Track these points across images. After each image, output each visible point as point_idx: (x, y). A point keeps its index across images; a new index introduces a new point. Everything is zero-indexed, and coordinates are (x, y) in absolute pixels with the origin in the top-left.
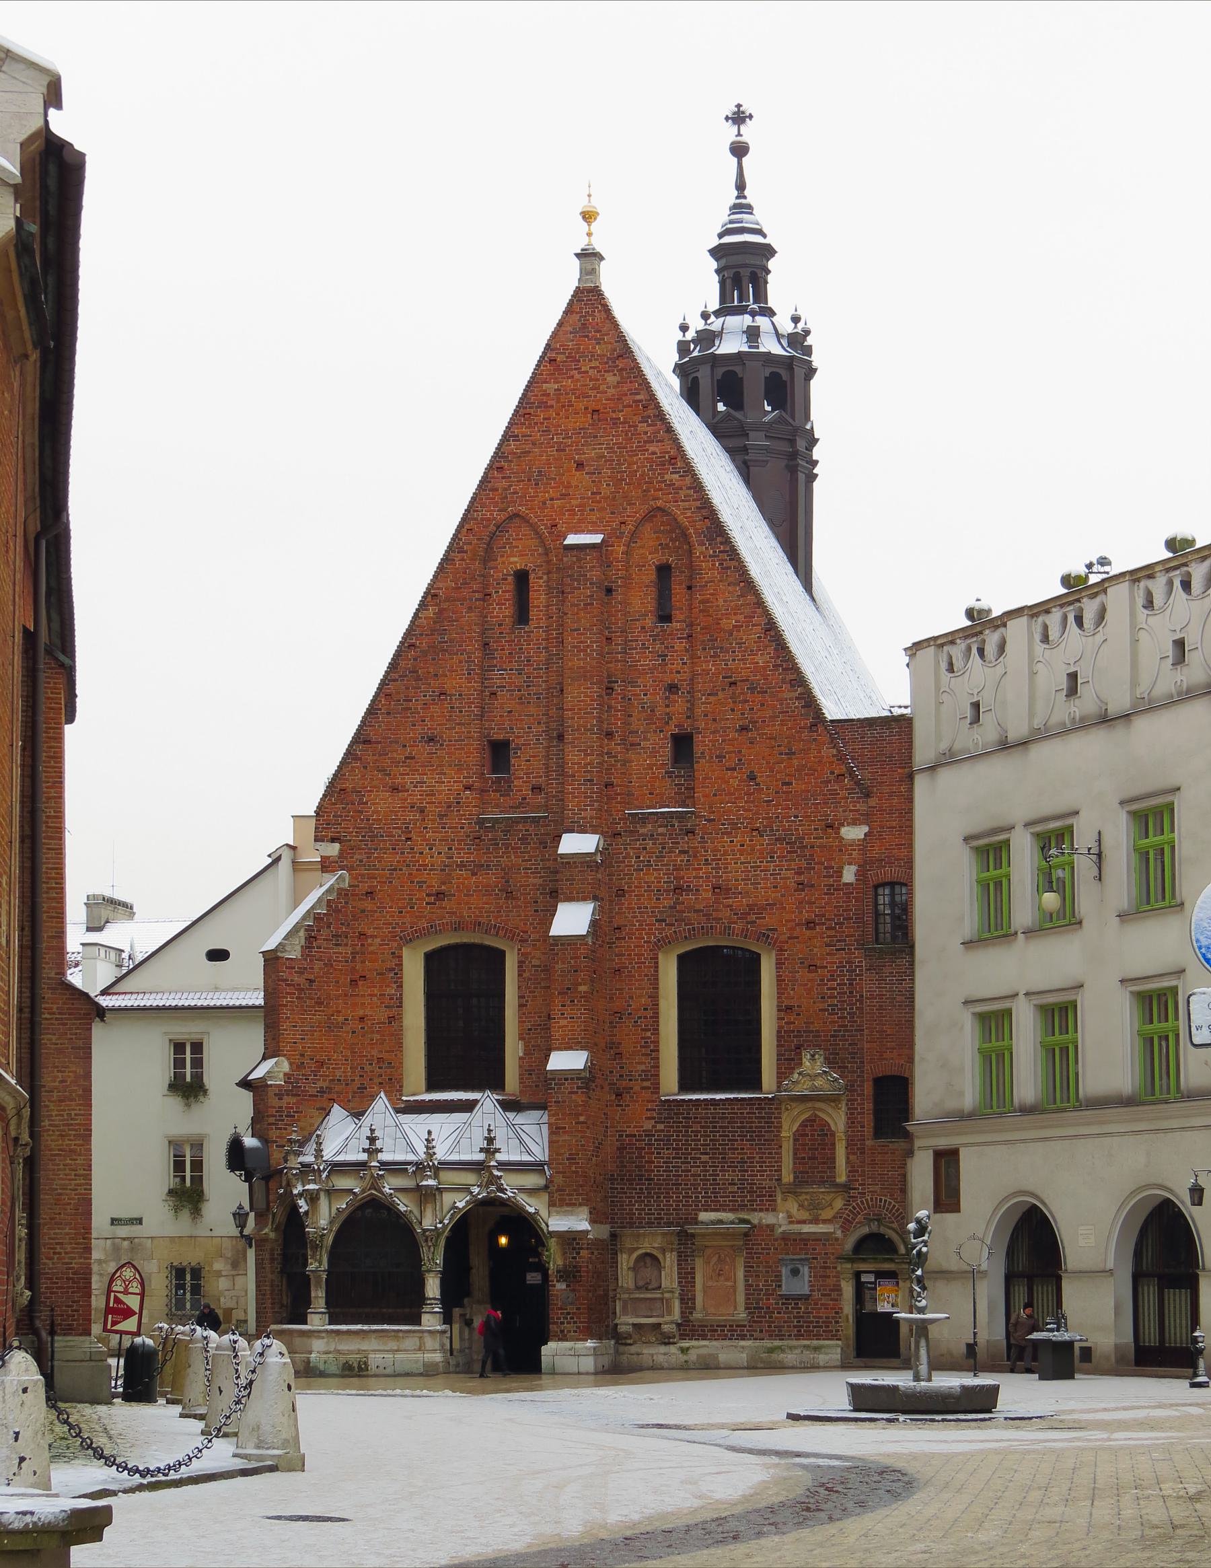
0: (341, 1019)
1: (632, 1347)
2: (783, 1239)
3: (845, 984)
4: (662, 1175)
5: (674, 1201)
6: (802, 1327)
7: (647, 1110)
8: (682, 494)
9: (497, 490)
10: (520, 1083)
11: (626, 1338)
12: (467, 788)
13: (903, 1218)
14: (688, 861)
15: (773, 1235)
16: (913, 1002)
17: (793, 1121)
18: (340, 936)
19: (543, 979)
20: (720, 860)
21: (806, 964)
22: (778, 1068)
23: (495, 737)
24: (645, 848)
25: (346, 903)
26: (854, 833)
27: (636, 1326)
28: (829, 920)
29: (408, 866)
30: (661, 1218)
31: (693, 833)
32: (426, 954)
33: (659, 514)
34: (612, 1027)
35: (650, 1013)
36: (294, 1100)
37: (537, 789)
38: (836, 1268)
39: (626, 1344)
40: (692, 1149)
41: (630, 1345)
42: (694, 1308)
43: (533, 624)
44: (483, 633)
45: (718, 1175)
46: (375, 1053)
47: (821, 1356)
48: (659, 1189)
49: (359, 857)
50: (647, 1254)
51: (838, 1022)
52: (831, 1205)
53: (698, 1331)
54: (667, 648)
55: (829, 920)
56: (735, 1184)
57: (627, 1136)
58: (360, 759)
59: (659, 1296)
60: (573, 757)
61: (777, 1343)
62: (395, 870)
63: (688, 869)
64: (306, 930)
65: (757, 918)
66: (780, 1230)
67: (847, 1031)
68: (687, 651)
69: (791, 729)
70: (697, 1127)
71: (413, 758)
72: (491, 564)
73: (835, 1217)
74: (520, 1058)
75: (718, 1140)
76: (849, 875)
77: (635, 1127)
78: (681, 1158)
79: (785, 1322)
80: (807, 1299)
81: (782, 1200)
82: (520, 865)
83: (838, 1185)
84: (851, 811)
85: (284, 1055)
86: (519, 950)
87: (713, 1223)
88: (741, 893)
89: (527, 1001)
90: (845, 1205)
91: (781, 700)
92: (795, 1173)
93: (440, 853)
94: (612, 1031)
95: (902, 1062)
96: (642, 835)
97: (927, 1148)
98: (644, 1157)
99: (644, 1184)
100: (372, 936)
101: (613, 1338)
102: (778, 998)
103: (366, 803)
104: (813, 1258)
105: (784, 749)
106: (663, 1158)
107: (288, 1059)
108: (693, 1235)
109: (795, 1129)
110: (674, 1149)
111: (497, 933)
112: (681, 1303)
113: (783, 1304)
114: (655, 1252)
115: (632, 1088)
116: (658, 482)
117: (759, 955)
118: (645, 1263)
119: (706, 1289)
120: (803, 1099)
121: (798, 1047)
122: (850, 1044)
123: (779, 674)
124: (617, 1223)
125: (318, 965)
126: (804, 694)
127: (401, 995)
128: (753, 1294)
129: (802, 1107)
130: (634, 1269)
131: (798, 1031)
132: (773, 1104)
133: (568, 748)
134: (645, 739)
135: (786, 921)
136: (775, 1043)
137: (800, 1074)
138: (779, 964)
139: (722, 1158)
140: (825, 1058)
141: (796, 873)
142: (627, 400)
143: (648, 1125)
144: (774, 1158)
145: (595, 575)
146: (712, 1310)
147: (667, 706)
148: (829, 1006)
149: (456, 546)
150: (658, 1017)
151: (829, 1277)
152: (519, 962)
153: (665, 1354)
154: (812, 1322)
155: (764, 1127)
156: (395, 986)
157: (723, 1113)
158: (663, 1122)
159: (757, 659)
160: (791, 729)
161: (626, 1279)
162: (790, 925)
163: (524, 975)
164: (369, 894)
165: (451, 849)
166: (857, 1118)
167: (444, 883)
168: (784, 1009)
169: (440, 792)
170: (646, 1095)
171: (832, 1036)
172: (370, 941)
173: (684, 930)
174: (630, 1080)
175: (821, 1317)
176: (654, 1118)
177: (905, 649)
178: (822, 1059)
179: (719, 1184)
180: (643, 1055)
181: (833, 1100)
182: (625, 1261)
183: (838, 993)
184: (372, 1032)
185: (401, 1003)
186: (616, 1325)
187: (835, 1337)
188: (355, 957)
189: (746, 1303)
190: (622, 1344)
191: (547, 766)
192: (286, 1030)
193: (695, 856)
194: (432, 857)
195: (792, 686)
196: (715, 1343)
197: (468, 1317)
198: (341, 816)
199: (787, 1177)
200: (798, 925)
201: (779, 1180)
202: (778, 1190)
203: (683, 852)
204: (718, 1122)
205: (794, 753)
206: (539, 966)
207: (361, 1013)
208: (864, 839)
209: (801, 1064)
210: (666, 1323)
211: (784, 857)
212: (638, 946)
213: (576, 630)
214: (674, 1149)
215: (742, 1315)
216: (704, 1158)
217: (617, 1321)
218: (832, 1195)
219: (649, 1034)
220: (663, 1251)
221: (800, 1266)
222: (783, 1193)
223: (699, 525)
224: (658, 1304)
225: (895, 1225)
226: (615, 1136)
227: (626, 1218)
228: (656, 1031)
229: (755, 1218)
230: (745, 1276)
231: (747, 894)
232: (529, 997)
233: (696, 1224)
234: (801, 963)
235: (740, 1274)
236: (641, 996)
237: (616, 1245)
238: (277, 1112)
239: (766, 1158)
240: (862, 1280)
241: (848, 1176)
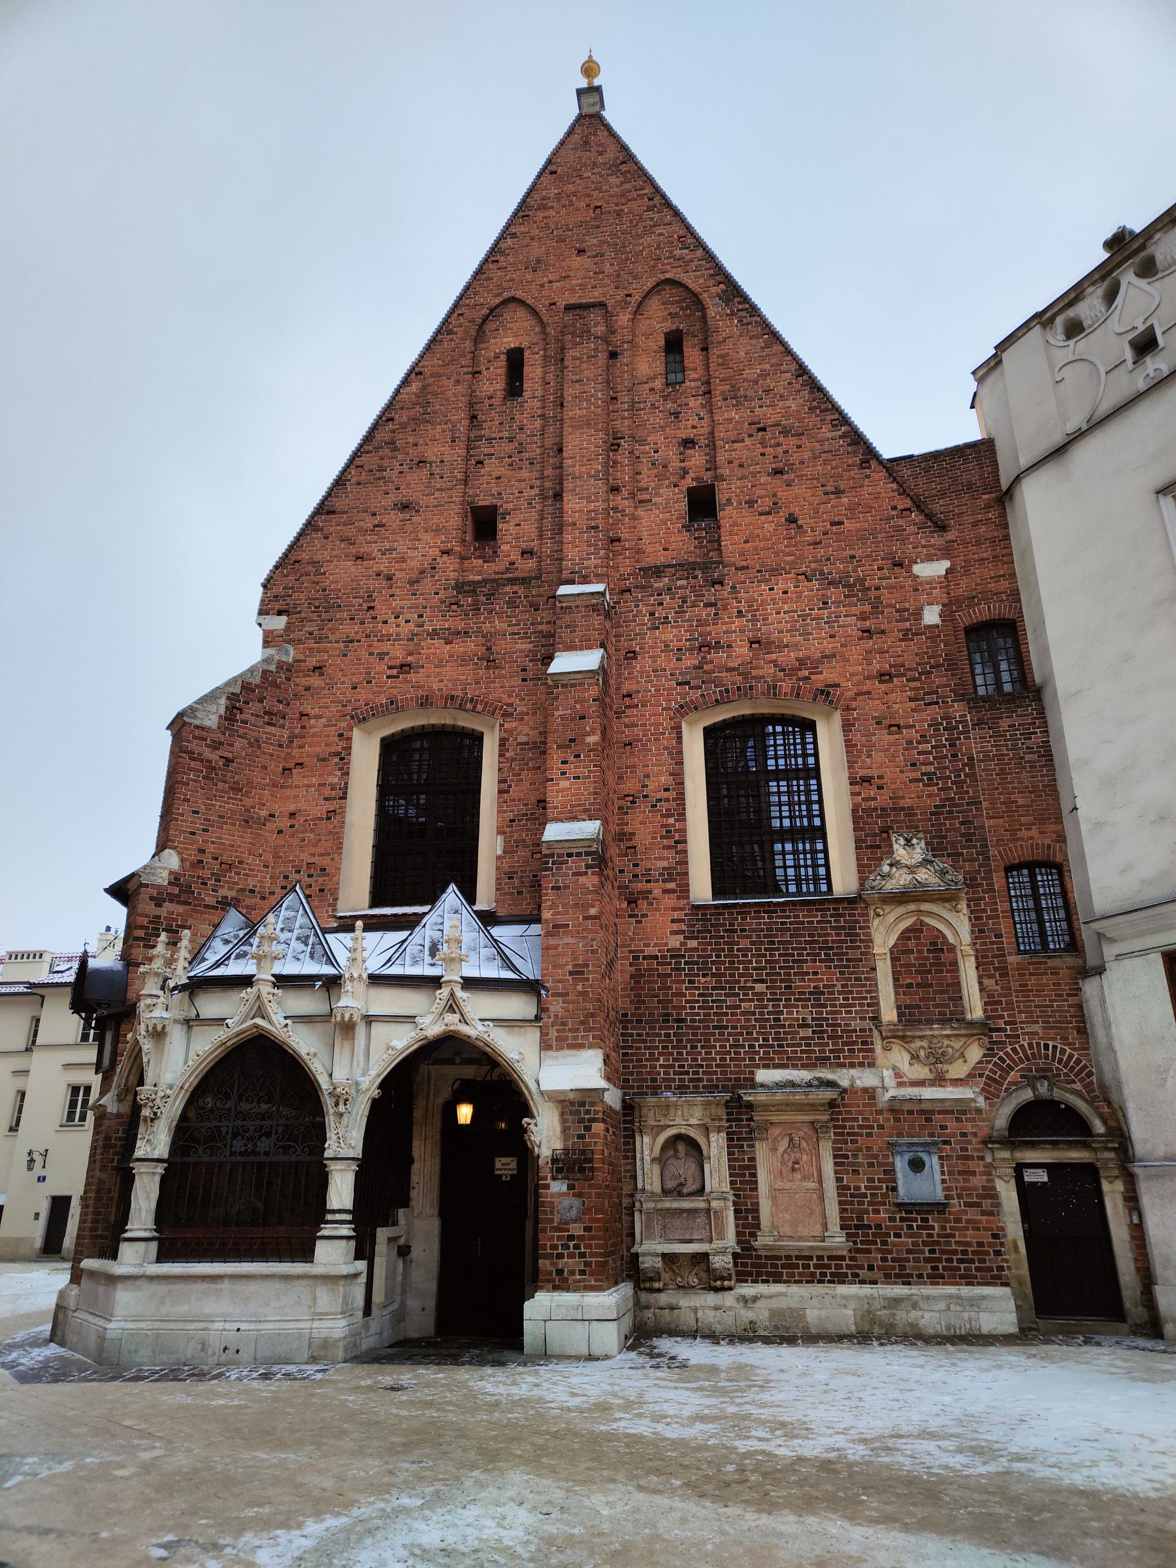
0: (264, 813)
1: (662, 1295)
2: (892, 1111)
3: (945, 746)
4: (698, 1014)
5: (717, 1053)
6: (939, 1260)
7: (673, 921)
8: (693, 265)
9: (491, 279)
10: (497, 889)
11: (651, 1279)
12: (447, 552)
13: (1090, 1074)
14: (715, 614)
15: (874, 1105)
16: (1052, 760)
17: (889, 930)
18: (275, 715)
19: (531, 759)
20: (758, 610)
21: (886, 722)
22: (858, 859)
23: (481, 503)
24: (661, 604)
25: (288, 679)
26: (932, 570)
27: (668, 1258)
28: (910, 670)
29: (368, 636)
30: (700, 1080)
31: (721, 583)
32: (383, 740)
33: (667, 287)
34: (621, 814)
35: (672, 794)
36: (180, 909)
37: (527, 553)
38: (982, 1158)
39: (652, 1290)
40: (741, 975)
41: (659, 1291)
42: (758, 1227)
43: (527, 395)
44: (471, 405)
45: (782, 1013)
46: (305, 857)
47: (983, 1317)
48: (694, 1034)
49: (310, 629)
50: (678, 1137)
51: (937, 795)
52: (962, 1055)
53: (765, 1266)
54: (680, 406)
55: (910, 670)
56: (808, 1026)
57: (645, 958)
58: (322, 530)
59: (702, 1205)
60: (572, 504)
61: (899, 1290)
62: (352, 641)
63: (717, 624)
64: (228, 698)
65: (810, 673)
66: (888, 1096)
67: (956, 805)
68: (703, 406)
69: (836, 468)
70: (744, 943)
71: (383, 526)
72: (482, 346)
73: (971, 1076)
74: (498, 858)
75: (778, 962)
76: (931, 616)
77: (656, 945)
78: (724, 988)
79: (909, 1251)
80: (943, 1212)
81: (886, 1049)
82: (505, 631)
83: (971, 1024)
84: (923, 546)
85: (174, 848)
86: (501, 725)
87: (779, 1085)
88: (787, 646)
89: (510, 786)
90: (985, 1056)
91: (821, 442)
92: (898, 1007)
93: (407, 621)
94: (622, 819)
95: (1047, 841)
96: (658, 589)
97: (1145, 952)
98: (670, 988)
99: (672, 1028)
100: (317, 717)
101: (629, 1277)
102: (849, 768)
103: (324, 573)
104: (945, 1142)
105: (829, 489)
106: (698, 988)
107: (179, 853)
108: (750, 1106)
109: (892, 942)
110: (713, 975)
111: (475, 707)
112: (736, 1218)
113: (902, 1219)
114: (693, 1133)
115: (650, 892)
116: (668, 258)
117: (814, 722)
118: (676, 1151)
119: (774, 1194)
120: (901, 898)
121: (885, 830)
122: (962, 823)
123: (817, 416)
124: (632, 1087)
125: (239, 743)
126: (848, 432)
127: (346, 783)
128: (852, 1203)
129: (901, 910)
130: (661, 1161)
131: (883, 809)
132: (856, 909)
133: (567, 497)
134: (657, 495)
135: (852, 675)
136: (851, 826)
137: (891, 865)
138: (847, 726)
139: (786, 987)
140: (926, 844)
141: (858, 619)
142: (634, 194)
143: (675, 942)
144: (865, 985)
145: (600, 329)
146: (786, 1230)
147: (683, 461)
148: (923, 774)
149: (445, 329)
150: (684, 799)
151: (974, 1173)
152: (500, 740)
153: (716, 1308)
154: (955, 1252)
155: (845, 942)
156: (339, 773)
157: (782, 923)
158: (697, 938)
159: (788, 403)
160: (836, 468)
161: (649, 1178)
162: (855, 679)
163: (507, 755)
164: (318, 669)
165: (420, 616)
166: (986, 924)
167: (411, 654)
168: (858, 781)
169: (413, 558)
170: (669, 901)
171: (932, 814)
172: (313, 721)
173: (715, 692)
174: (648, 881)
175: (969, 1244)
176: (683, 932)
177: (974, 373)
178: (923, 844)
179: (784, 1026)
180: (665, 848)
181: (947, 898)
182: (647, 1147)
183: (934, 758)
184: (305, 831)
185: (345, 793)
186: (637, 1255)
187: (997, 1278)
188: (292, 742)
189: (841, 1218)
190: (645, 1289)
191: (541, 530)
192: (183, 815)
193: (725, 608)
194: (398, 626)
195: (834, 426)
196: (794, 1289)
197: (402, 1241)
198: (292, 588)
199: (889, 1014)
200: (869, 678)
201: (876, 1019)
202: (876, 1033)
203: (707, 605)
204: (776, 936)
205: (843, 492)
206: (526, 743)
207: (292, 808)
208: (946, 577)
209: (891, 852)
210: (718, 1253)
211: (840, 602)
212: (655, 715)
213: (577, 381)
214: (713, 975)
215: (837, 1240)
216: (760, 988)
217: (636, 1249)
218: (963, 1040)
219: (671, 821)
220: (706, 1130)
221: (925, 1156)
222: (883, 1039)
223: (713, 290)
224: (701, 1220)
225: (1078, 1086)
226: (627, 958)
227: (646, 1080)
228: (682, 816)
229: (844, 1077)
230: (836, 1172)
231: (796, 646)
232: (512, 780)
233: (753, 1086)
234: (877, 723)
235: (828, 1167)
236: (659, 774)
237: (632, 1122)
238: (150, 922)
239: (852, 986)
240: (1026, 1179)
241: (985, 1011)
